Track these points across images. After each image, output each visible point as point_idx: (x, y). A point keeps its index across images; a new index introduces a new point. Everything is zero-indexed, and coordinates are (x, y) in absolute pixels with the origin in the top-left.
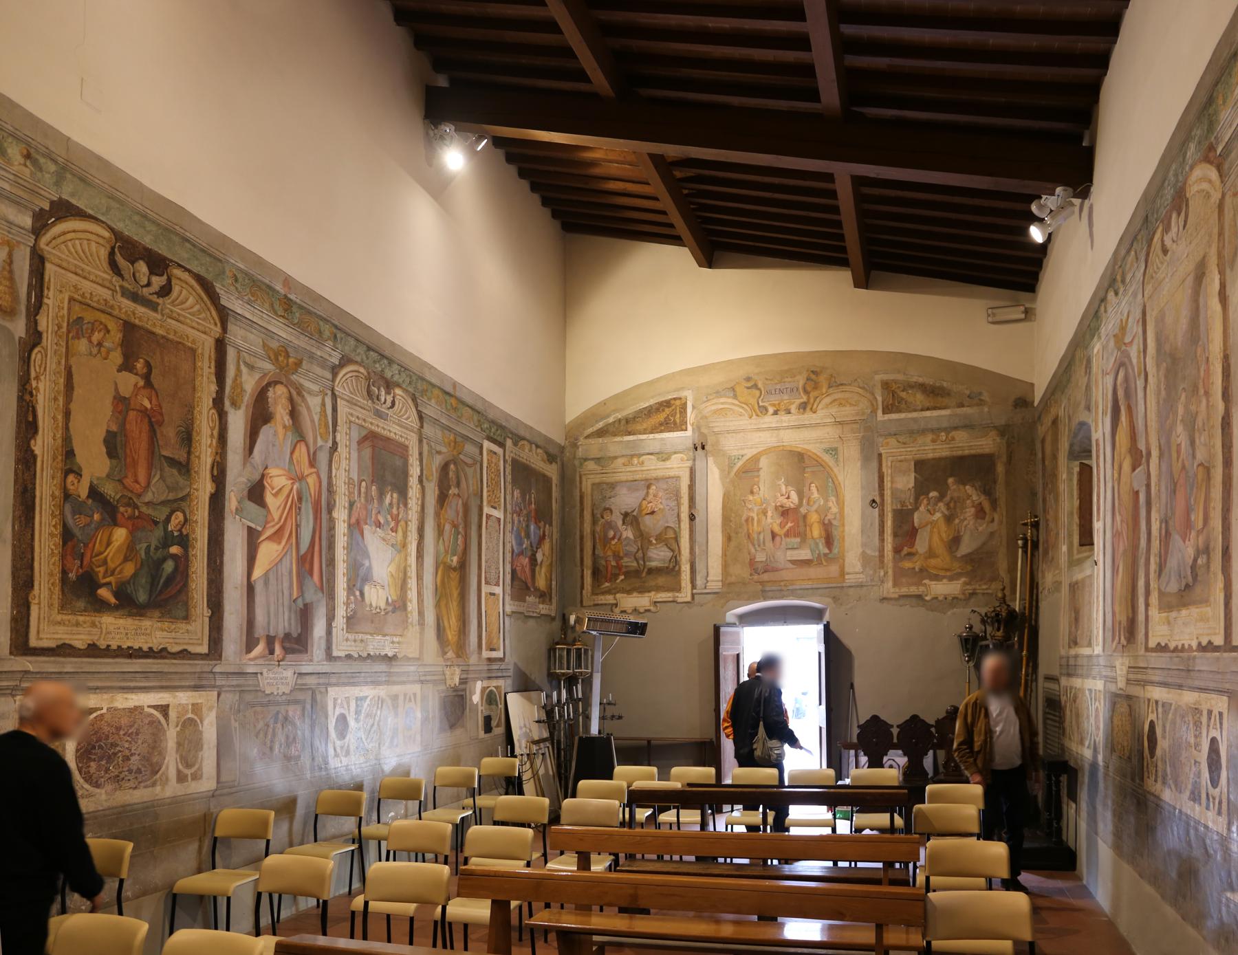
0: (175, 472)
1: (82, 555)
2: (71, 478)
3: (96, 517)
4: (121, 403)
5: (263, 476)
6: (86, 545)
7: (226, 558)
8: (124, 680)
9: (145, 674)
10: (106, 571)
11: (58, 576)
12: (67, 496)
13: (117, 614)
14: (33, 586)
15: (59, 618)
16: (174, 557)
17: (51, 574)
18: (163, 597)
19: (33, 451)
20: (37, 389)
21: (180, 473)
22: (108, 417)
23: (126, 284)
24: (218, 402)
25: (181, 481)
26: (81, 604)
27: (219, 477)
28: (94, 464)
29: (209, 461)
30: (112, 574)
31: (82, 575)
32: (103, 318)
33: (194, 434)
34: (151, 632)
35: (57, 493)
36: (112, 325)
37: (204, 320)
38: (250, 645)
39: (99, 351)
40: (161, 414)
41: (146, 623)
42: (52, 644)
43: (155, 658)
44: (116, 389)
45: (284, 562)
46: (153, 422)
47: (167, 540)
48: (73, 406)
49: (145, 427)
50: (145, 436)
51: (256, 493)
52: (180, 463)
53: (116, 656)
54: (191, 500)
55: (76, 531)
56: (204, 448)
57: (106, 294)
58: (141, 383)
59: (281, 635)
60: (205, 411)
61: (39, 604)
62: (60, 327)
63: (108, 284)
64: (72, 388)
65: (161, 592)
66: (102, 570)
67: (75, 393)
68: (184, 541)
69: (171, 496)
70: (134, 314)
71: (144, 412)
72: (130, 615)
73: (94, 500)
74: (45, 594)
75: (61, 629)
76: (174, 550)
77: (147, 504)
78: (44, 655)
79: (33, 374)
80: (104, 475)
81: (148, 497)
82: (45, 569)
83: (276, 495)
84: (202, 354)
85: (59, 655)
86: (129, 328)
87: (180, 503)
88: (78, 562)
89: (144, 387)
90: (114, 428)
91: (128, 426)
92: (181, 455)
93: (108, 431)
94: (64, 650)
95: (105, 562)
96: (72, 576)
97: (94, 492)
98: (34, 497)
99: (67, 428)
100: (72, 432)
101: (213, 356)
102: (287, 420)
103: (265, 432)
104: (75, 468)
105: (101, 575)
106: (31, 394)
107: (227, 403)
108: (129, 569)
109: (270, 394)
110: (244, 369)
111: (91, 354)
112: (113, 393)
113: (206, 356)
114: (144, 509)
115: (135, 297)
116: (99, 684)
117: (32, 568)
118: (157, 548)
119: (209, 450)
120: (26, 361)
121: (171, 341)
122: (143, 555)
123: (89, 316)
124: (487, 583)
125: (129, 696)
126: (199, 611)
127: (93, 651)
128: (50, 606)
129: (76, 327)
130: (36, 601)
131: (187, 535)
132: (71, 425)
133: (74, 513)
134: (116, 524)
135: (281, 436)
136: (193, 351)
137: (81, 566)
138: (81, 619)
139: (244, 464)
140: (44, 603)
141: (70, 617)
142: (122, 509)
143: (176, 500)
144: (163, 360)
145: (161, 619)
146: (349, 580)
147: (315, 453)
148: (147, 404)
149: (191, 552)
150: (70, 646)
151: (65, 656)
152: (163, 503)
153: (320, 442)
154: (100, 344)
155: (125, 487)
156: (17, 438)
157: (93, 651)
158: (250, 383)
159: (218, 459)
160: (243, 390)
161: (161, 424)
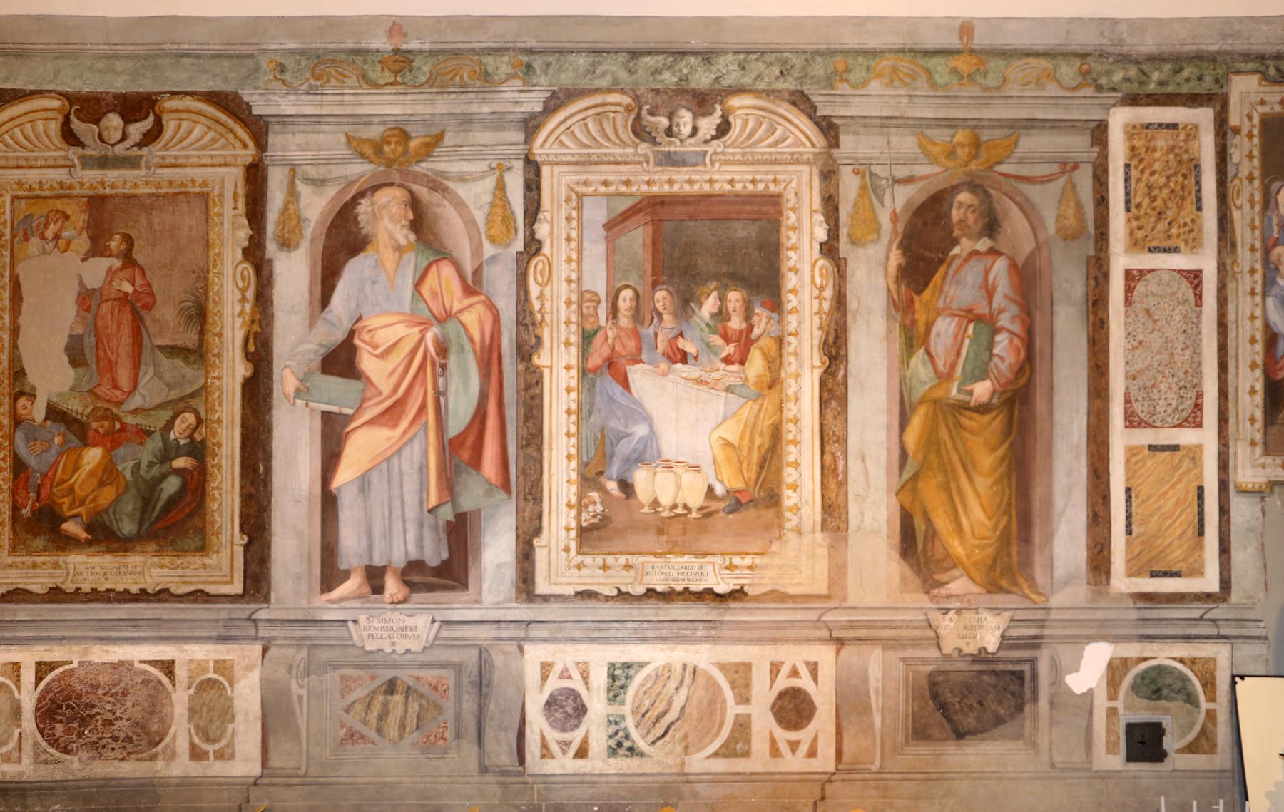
0: (178, 362)
2: (22, 401)
4: (86, 299)
5: (352, 333)
7: (277, 463)
8: (102, 629)
9: (133, 622)
10: (74, 500)
12: (17, 422)
13: (91, 550)
15: (10, 560)
16: (180, 472)
18: (159, 525)
21: (186, 360)
22: (71, 320)
23: (88, 152)
24: (255, 253)
25: (189, 372)
26: (39, 542)
27: (259, 354)
29: (240, 336)
30: (82, 503)
31: (40, 509)
32: (59, 205)
33: (210, 305)
34: (144, 568)
36: (71, 208)
37: (223, 148)
38: (331, 576)
39: (56, 246)
40: (152, 294)
41: (135, 559)
43: (149, 601)
44: (81, 283)
45: (407, 452)
46: (137, 308)
47: (166, 455)
48: (22, 320)
49: (127, 316)
50: (126, 330)
51: (341, 361)
52: (187, 350)
53: (90, 601)
54: (208, 394)
55: (32, 461)
56: (227, 320)
57: (60, 175)
58: (117, 263)
59: (399, 560)
60: (228, 270)
63: (62, 162)
64: (21, 299)
65: (158, 519)
67: (25, 305)
68: (199, 450)
69: (174, 395)
70: (102, 183)
71: (124, 299)
72: (109, 551)
76: (180, 463)
77: (134, 412)
80: (67, 389)
81: (136, 402)
83: (383, 356)
84: (221, 195)
86: (97, 203)
87: (192, 400)
88: (33, 495)
89: (122, 269)
91: (100, 323)
92: (189, 338)
93: (71, 337)
95: (71, 490)
96: (26, 512)
97: (54, 413)
99: (14, 346)
101: (241, 191)
102: (403, 236)
103: (354, 272)
104: (27, 389)
105: (65, 507)
107: (271, 248)
108: (107, 496)
109: (364, 208)
110: (301, 187)
111: (44, 252)
112: (76, 288)
113: (229, 195)
114: (130, 420)
115: (103, 163)
116: (66, 634)
118: (151, 465)
119: (239, 321)
121: (165, 196)
122: (128, 476)
123: (41, 210)
124: (1132, 421)
125: (111, 648)
126: (224, 538)
127: (56, 595)
131: (203, 442)
134: (86, 444)
135: (390, 265)
136: (204, 197)
137: (38, 500)
138: (39, 560)
139: (312, 325)
141: (24, 559)
142: (94, 425)
143: (181, 399)
144: (150, 224)
145: (158, 553)
146: (583, 465)
147: (477, 272)
148: (128, 288)
149: (210, 462)
150: (26, 591)
151: (17, 602)
152: (159, 407)
153: (489, 250)
154: (57, 237)
155: (98, 397)
157: (56, 595)
158: (316, 207)
159: (256, 328)
160: (300, 220)
161: (149, 307)
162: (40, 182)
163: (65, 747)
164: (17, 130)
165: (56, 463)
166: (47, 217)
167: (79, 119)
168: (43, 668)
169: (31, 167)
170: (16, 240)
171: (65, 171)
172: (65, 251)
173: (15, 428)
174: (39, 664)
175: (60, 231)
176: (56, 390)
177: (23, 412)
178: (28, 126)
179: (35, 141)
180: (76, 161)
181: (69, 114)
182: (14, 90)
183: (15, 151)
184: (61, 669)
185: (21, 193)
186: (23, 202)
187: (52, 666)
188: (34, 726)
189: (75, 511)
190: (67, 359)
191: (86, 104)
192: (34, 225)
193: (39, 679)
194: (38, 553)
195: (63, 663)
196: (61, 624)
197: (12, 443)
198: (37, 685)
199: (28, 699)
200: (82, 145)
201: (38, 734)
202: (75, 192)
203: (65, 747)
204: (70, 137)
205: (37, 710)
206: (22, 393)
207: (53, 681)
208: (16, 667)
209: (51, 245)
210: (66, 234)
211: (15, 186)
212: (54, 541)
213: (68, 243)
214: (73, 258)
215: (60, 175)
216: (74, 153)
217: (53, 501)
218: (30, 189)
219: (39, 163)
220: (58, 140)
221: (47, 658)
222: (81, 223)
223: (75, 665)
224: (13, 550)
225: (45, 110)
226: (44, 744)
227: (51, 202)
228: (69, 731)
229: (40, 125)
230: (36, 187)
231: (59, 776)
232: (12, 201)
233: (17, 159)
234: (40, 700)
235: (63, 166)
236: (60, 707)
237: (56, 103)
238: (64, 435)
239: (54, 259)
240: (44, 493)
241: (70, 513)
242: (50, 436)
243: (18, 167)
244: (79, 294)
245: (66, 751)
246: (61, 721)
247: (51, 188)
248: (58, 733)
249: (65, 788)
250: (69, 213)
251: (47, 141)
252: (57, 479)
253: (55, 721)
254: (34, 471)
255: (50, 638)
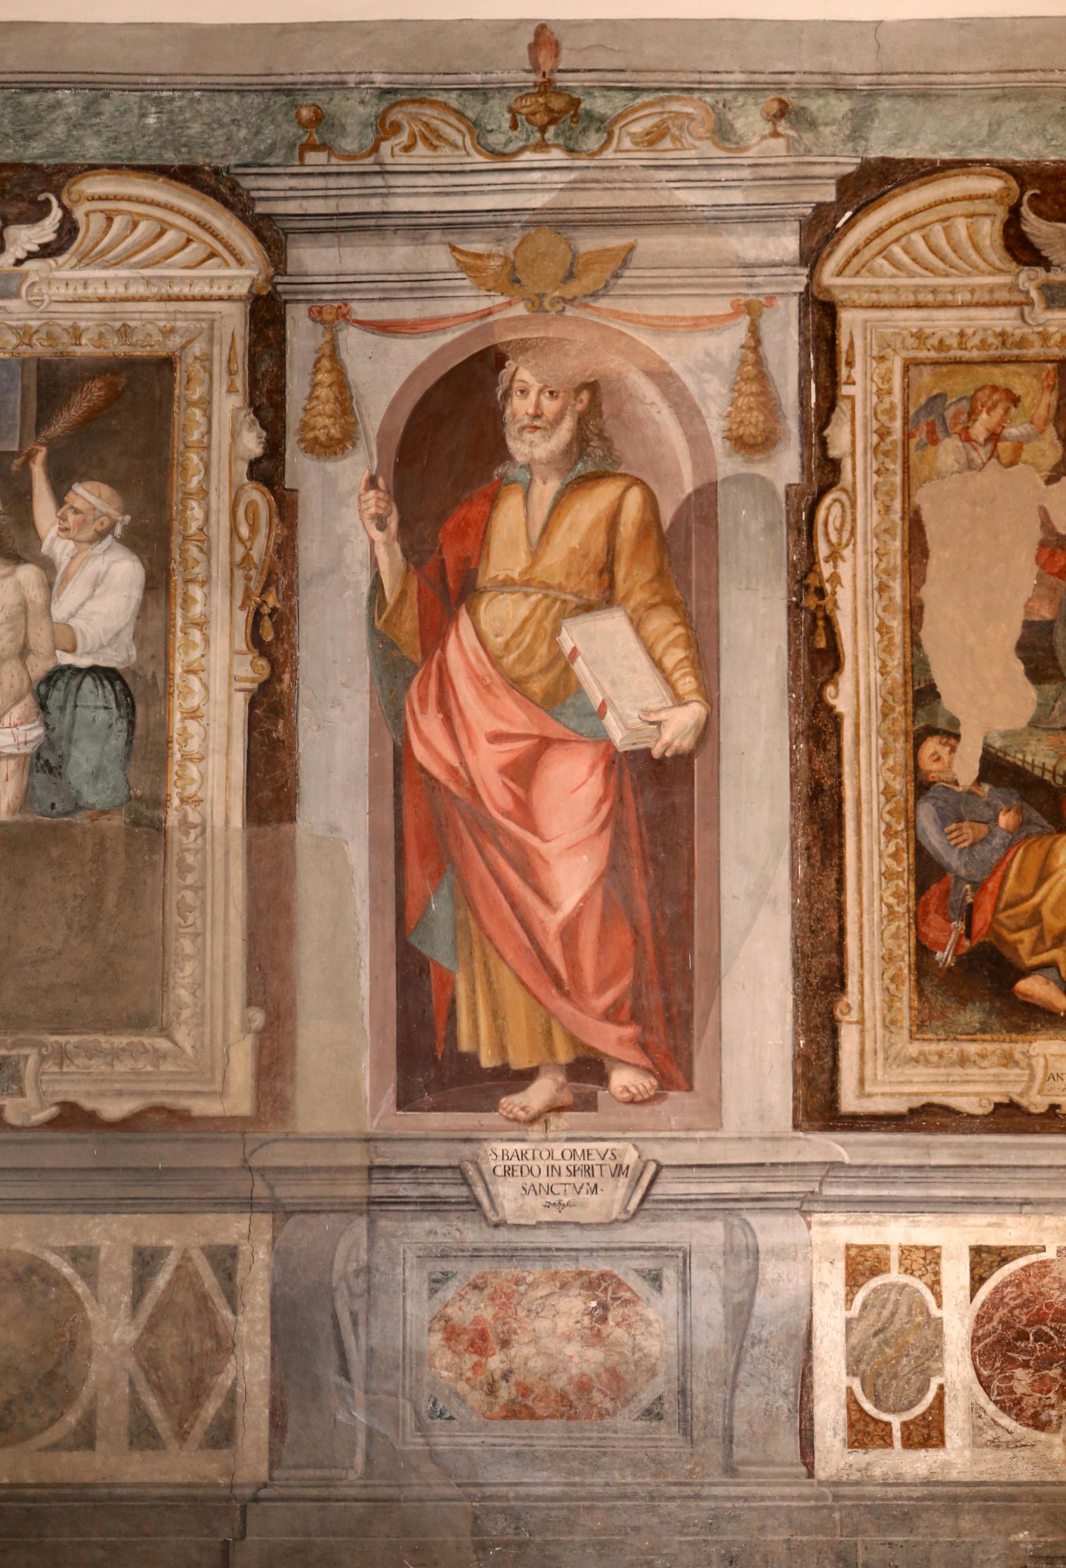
1: (969, 914)
2: (931, 746)
3: (1005, 820)
6: (979, 887)
10: (1041, 938)
11: (905, 963)
12: (922, 786)
14: (843, 987)
15: (914, 1049)
17: (889, 958)
19: (831, 709)
20: (835, 579)
22: (1028, 593)
26: (972, 1016)
28: (991, 701)
31: (972, 953)
32: (998, 376)
35: (898, 785)
36: (1022, 382)
39: (994, 454)
42: (900, 1106)
44: (1046, 523)
48: (928, 593)
55: (953, 861)
57: (1004, 319)
61: (861, 1022)
62: (883, 433)
63: (1004, 296)
64: (925, 553)
66: (1027, 937)
67: (933, 563)
73: (996, 784)
74: (875, 998)
75: (921, 1072)
78: (878, 1130)
79: (823, 550)
80: (1022, 723)
82: (873, 948)
85: (916, 1129)
88: (959, 926)
90: (1045, 612)
93: (1028, 625)
94: (928, 1117)
95: (1035, 918)
97: (995, 767)
98: (840, 802)
99: (915, 642)
100: (928, 646)
104: (942, 724)
105: (1024, 949)
106: (821, 593)
111: (970, 465)
112: (1037, 535)
116: (1031, 1193)
117: (841, 949)
120: (804, 529)
123: (959, 385)
127: (1009, 1117)
128: (890, 1024)
129: (928, 420)
130: (854, 1016)
132: (924, 634)
133: (943, 820)
137: (968, 934)
138: (972, 1049)
140: (874, 1019)
141: (942, 1046)
150: (947, 1110)
154: (994, 437)
156: (791, 690)
157: (1009, 1117)
162: (962, 334)
163: (1035, 1416)
164: (916, 237)
165: (1001, 866)
166: (973, 399)
167: (1039, 214)
168: (984, 1260)
169: (943, 306)
170: (913, 442)
171: (1013, 312)
172: (1012, 464)
173: (917, 798)
174: (977, 1251)
175: (1001, 424)
176: (1001, 726)
177: (935, 767)
178: (938, 228)
179: (952, 256)
180: (1034, 294)
181: (1019, 204)
182: (911, 161)
183: (911, 275)
184: (1022, 1262)
185: (923, 354)
186: (927, 371)
187: (1003, 1255)
188: (972, 1374)
189: (1045, 957)
190: (1020, 667)
191: (1051, 186)
192: (949, 414)
193: (977, 1282)
194: (971, 1034)
195: (1025, 1251)
196: (1021, 1174)
197: (912, 824)
198: (973, 1292)
199: (957, 1317)
200: (1045, 263)
201: (977, 1388)
202: (1030, 353)
203: (1035, 1416)
204: (1020, 248)
205: (975, 1340)
206: (931, 731)
207: (1005, 1284)
208: (932, 1255)
209: (983, 453)
210: (1013, 431)
211: (911, 342)
212: (1000, 1013)
213: (1019, 447)
214: (1027, 479)
215: (1004, 319)
216: (1029, 279)
217: (999, 937)
218: (941, 346)
219: (959, 298)
220: (996, 255)
221: (993, 1239)
222: (1042, 411)
223: (1050, 1254)
224: (920, 1027)
225: (971, 198)
226: (991, 1408)
227: (980, 369)
228: (1042, 1385)
229: (961, 226)
230: (954, 342)
231: (1024, 1472)
232: (906, 369)
233: (916, 290)
234: (979, 1319)
235: (1008, 304)
236: (1023, 1336)
237: (993, 185)
238: (1020, 811)
239: (992, 476)
240: (980, 921)
241: (1035, 961)
242: (988, 813)
243: (918, 306)
244: (1042, 545)
245: (1038, 1423)
246: (1026, 1365)
247: (983, 345)
248: (1020, 1388)
249: (1039, 1499)
250: (1018, 391)
251: (975, 257)
252: (1006, 896)
253: (1012, 1361)
254: (958, 878)
255: (998, 1202)
